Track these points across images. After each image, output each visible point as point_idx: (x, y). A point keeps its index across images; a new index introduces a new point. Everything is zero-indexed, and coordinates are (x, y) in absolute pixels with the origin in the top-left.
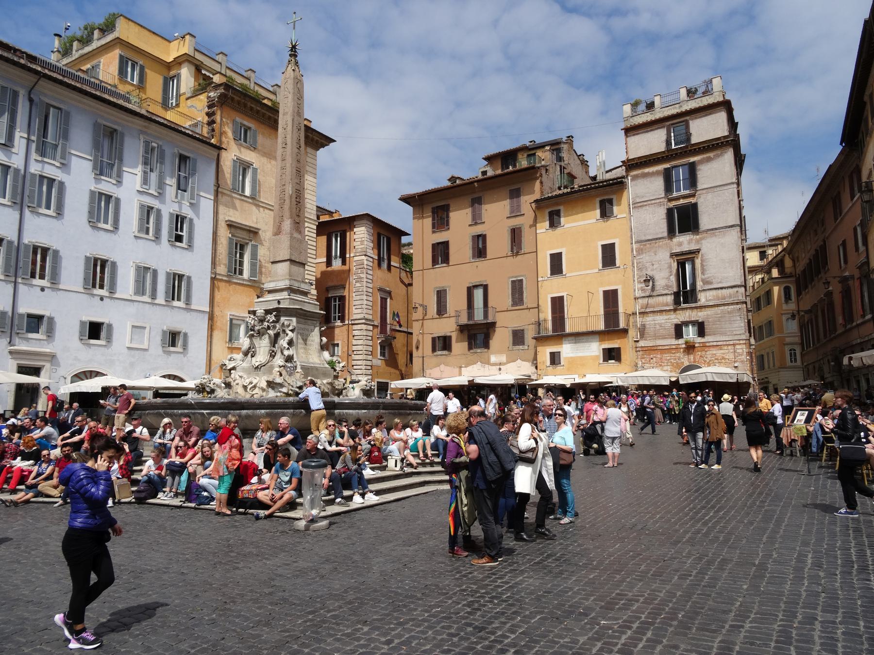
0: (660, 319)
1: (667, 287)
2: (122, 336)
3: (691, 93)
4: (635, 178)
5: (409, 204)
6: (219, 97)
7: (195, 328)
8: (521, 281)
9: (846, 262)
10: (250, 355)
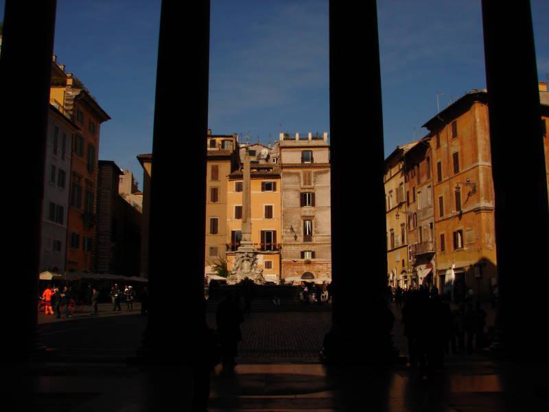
3: (313, 138)
6: (76, 96)
8: (217, 219)
10: (239, 269)
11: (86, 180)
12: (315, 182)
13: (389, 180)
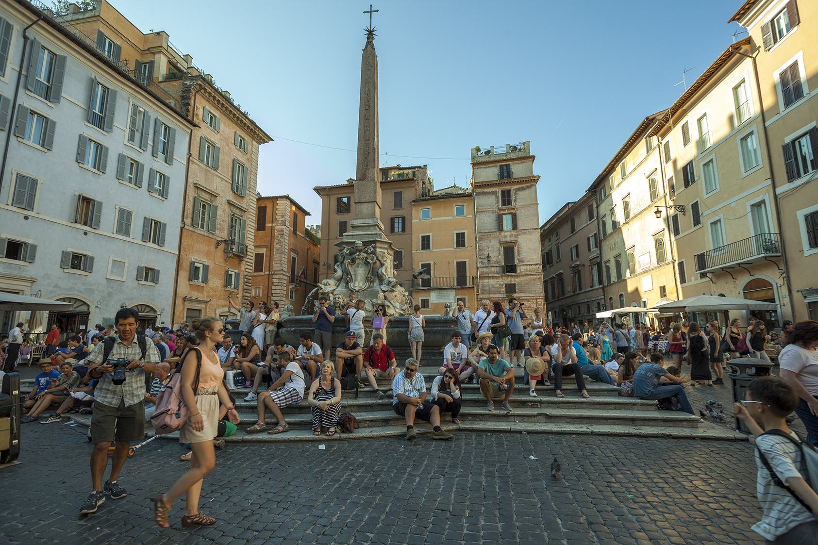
0: (492, 281)
1: (497, 262)
2: (102, 268)
4: (478, 194)
5: (319, 194)
7: (166, 267)
9: (577, 256)
11: (229, 203)
12: (515, 201)
13: (618, 185)
